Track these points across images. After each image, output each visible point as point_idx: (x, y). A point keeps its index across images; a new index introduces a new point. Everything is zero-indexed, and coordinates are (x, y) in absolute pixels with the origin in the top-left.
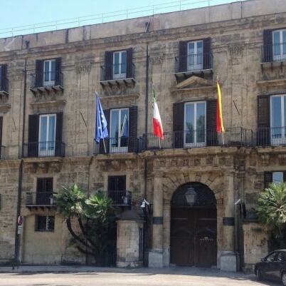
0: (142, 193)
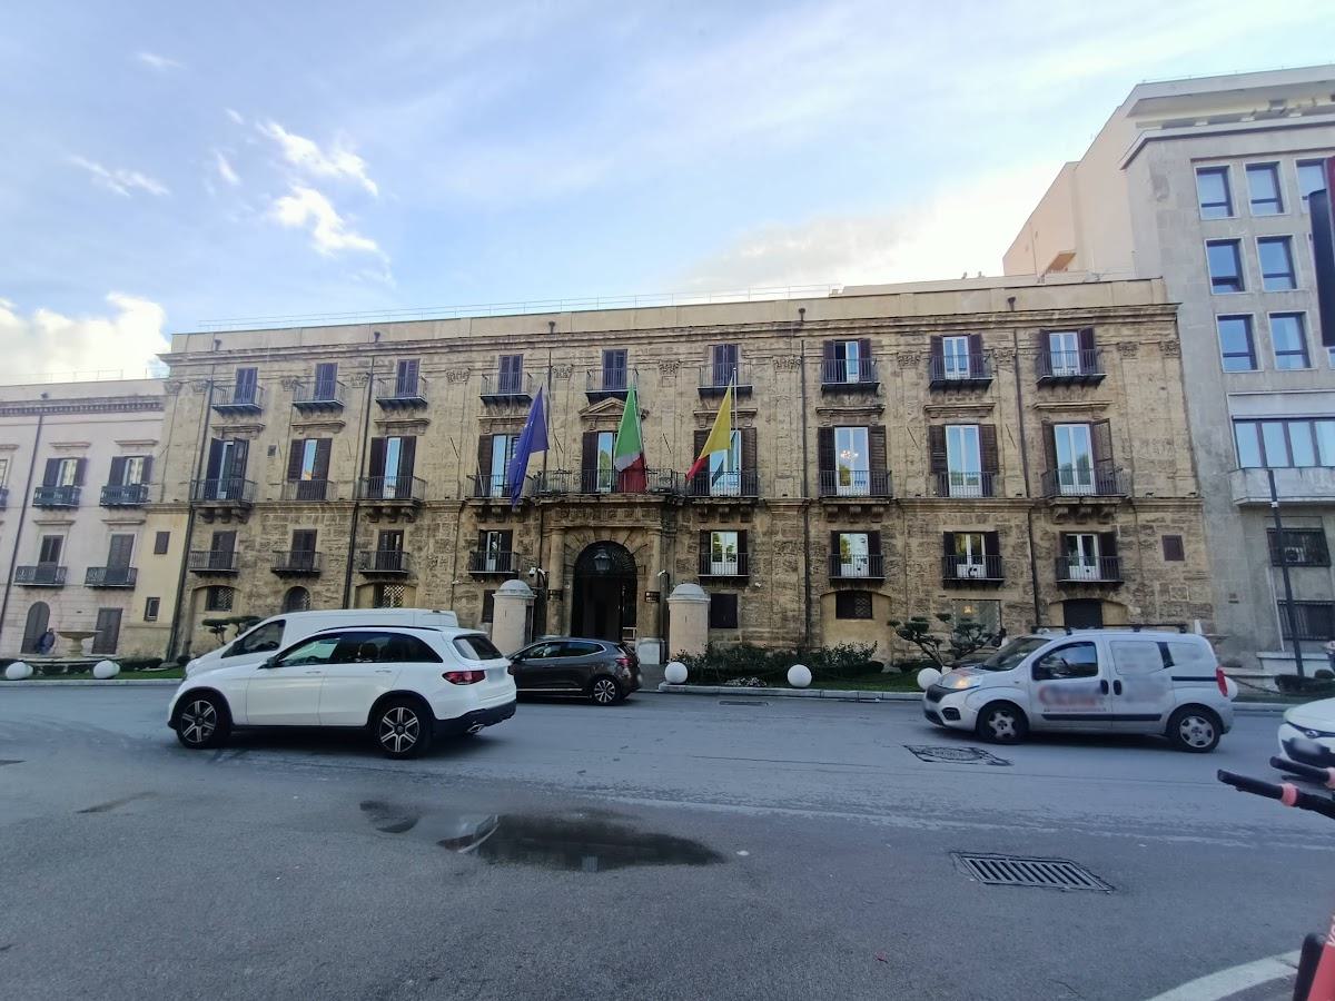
0: (535, 554)
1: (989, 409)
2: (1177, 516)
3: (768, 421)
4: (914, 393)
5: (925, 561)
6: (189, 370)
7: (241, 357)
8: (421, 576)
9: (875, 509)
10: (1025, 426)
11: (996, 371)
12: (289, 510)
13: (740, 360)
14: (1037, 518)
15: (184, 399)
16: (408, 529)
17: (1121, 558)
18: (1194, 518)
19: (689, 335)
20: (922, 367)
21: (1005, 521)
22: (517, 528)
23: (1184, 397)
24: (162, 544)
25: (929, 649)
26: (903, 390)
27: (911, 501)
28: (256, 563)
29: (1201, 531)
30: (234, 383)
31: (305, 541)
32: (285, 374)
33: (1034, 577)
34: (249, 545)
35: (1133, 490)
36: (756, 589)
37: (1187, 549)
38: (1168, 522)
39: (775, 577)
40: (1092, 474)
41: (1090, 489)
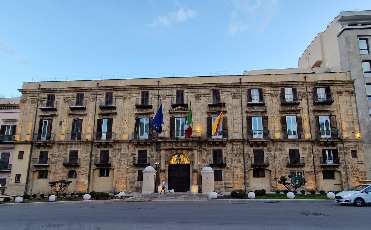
0: (155, 158)
1: (299, 111)
2: (355, 144)
3: (231, 114)
4: (276, 106)
5: (281, 159)
6: (29, 95)
7: (49, 91)
8: (116, 165)
9: (265, 143)
10: (310, 116)
11: (301, 99)
12: (68, 143)
13: (221, 95)
14: (314, 145)
15: (28, 105)
16: (111, 150)
17: (339, 157)
18: (360, 145)
19: (204, 86)
20: (278, 97)
21: (305, 146)
22: (148, 149)
23: (357, 108)
24: (21, 156)
25: (287, 186)
26: (273, 104)
27: (276, 140)
28: (56, 162)
29: (362, 149)
30: (46, 100)
31: (74, 154)
32: (65, 97)
33: (314, 163)
34: (53, 156)
35: (342, 137)
36: (228, 168)
37: (358, 154)
38: (353, 146)
39: (234, 164)
40: (330, 132)
41: (329, 136)
